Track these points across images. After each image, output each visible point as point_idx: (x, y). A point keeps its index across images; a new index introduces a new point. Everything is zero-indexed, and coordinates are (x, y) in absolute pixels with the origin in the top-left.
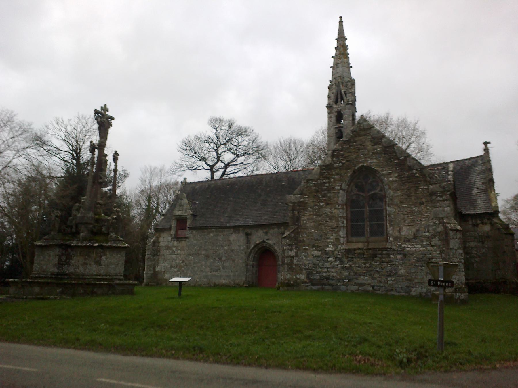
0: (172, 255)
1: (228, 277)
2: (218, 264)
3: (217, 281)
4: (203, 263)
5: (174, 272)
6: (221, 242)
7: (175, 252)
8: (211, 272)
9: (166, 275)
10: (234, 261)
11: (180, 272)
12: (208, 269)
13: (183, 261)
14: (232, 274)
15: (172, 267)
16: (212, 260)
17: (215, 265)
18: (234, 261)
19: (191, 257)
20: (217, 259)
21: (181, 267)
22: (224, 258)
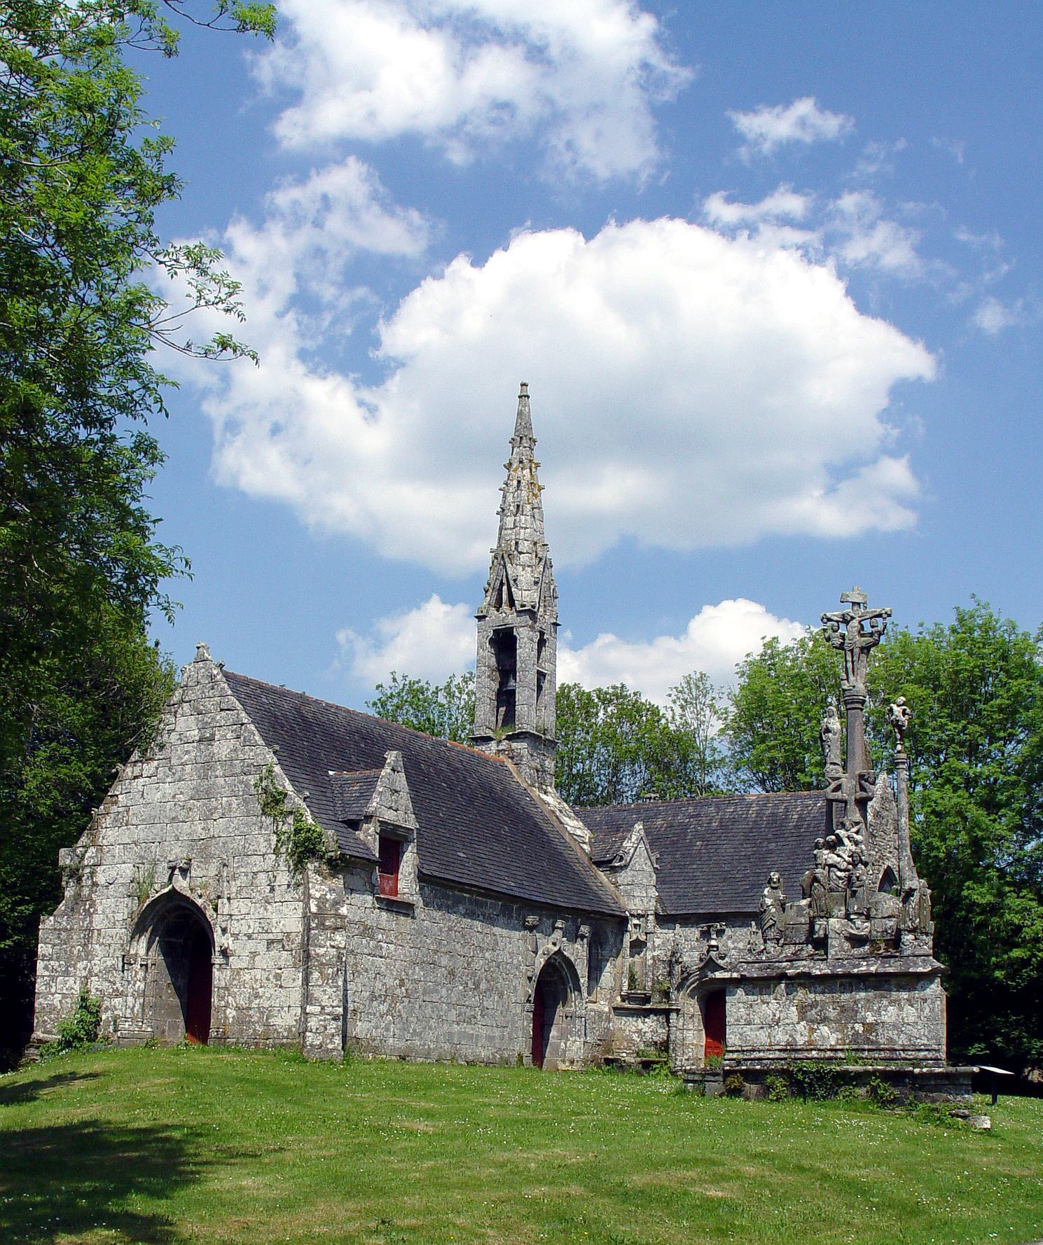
0: (374, 956)
1: (491, 1039)
2: (475, 1001)
3: (468, 1051)
4: (444, 992)
5: (378, 1014)
6: (480, 936)
7: (381, 948)
8: (458, 1024)
9: (359, 1024)
10: (501, 995)
11: (393, 1016)
12: (453, 1015)
13: (402, 984)
14: (497, 1033)
15: (373, 997)
16: (461, 988)
17: (467, 1003)
18: (501, 995)
19: (418, 973)
20: (470, 985)
21: (395, 998)
22: (483, 986)
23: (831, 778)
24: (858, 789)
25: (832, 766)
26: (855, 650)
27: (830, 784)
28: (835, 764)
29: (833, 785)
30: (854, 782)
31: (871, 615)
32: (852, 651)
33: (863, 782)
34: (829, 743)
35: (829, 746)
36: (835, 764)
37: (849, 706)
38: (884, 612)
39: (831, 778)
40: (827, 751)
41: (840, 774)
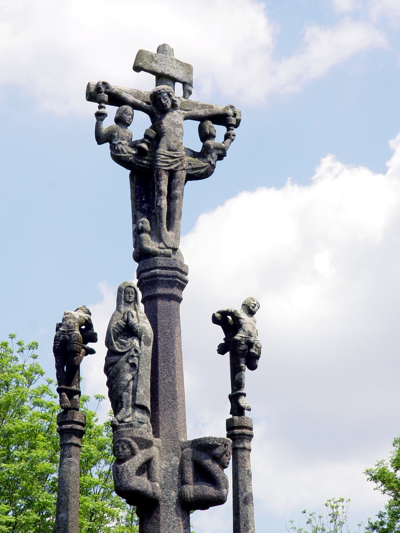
23: (135, 439)
24: (189, 475)
25: (138, 414)
26: (179, 173)
27: (133, 454)
28: (143, 408)
29: (140, 457)
30: (176, 461)
31: (208, 112)
32: (172, 174)
33: (209, 462)
34: (136, 360)
35: (133, 365)
36: (143, 408)
37: (160, 291)
38: (230, 112)
39: (133, 438)
40: (129, 377)
41: (150, 436)
